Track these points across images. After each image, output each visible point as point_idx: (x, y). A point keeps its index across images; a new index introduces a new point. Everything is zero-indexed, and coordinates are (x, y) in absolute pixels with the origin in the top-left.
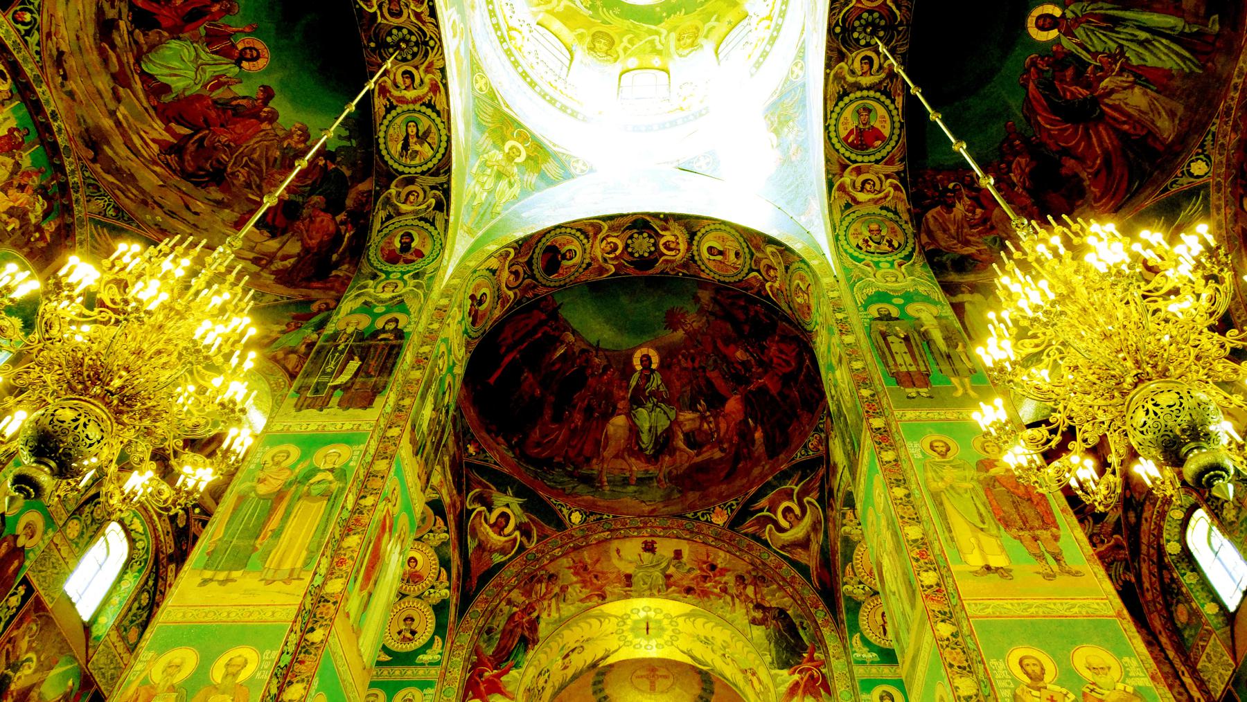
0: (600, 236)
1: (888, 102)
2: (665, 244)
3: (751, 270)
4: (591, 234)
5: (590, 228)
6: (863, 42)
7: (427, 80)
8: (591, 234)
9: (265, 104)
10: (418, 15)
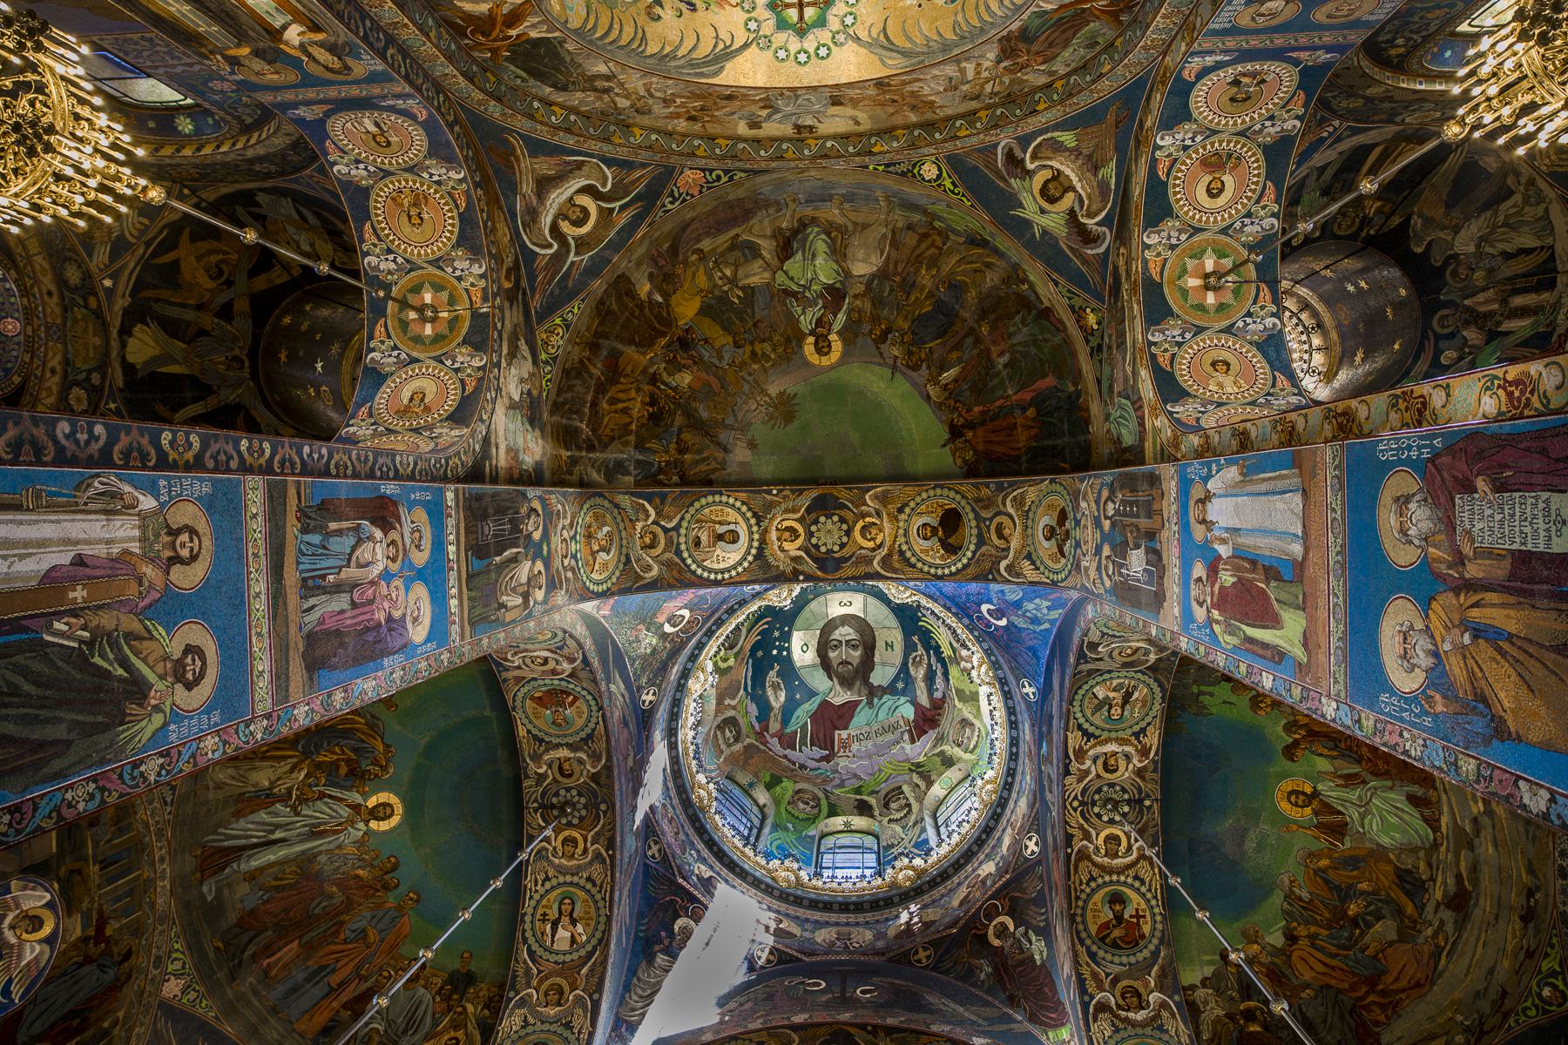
0: (884, 551)
1: (534, 731)
2: (797, 537)
3: (677, 528)
4: (896, 557)
5: (897, 565)
6: (574, 792)
7: (1088, 763)
8: (896, 557)
9: (1296, 743)
10: (1087, 836)
